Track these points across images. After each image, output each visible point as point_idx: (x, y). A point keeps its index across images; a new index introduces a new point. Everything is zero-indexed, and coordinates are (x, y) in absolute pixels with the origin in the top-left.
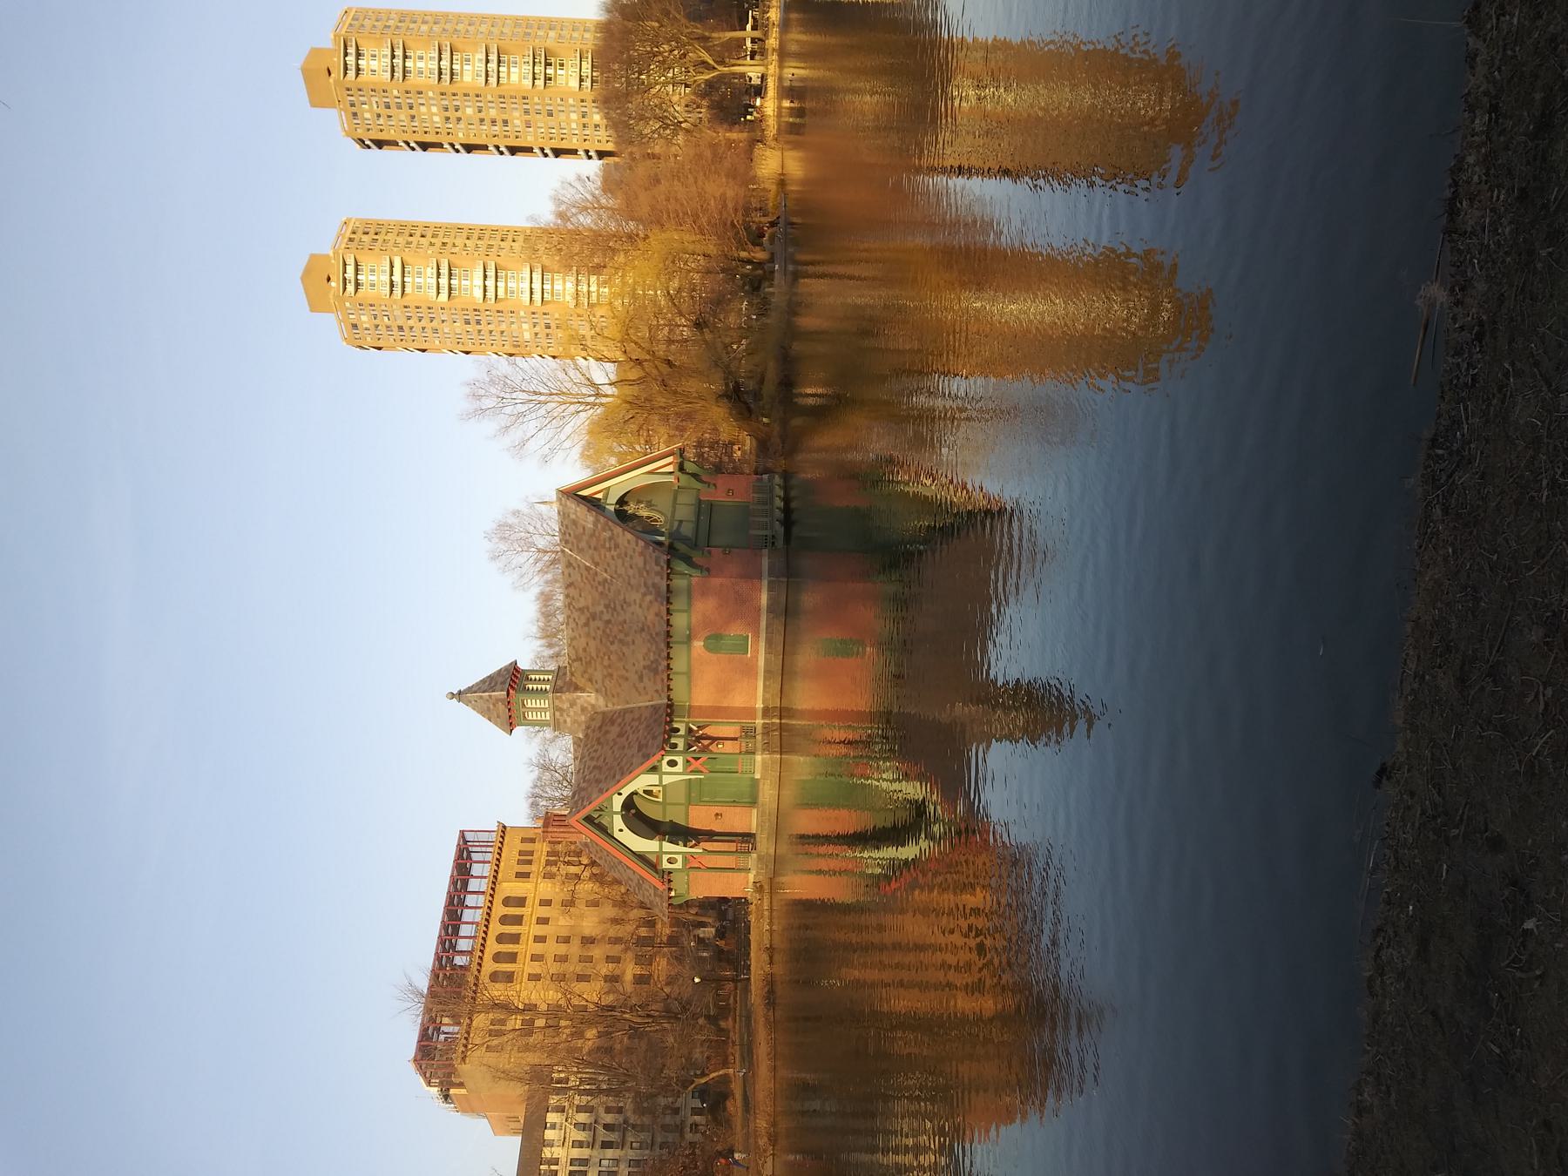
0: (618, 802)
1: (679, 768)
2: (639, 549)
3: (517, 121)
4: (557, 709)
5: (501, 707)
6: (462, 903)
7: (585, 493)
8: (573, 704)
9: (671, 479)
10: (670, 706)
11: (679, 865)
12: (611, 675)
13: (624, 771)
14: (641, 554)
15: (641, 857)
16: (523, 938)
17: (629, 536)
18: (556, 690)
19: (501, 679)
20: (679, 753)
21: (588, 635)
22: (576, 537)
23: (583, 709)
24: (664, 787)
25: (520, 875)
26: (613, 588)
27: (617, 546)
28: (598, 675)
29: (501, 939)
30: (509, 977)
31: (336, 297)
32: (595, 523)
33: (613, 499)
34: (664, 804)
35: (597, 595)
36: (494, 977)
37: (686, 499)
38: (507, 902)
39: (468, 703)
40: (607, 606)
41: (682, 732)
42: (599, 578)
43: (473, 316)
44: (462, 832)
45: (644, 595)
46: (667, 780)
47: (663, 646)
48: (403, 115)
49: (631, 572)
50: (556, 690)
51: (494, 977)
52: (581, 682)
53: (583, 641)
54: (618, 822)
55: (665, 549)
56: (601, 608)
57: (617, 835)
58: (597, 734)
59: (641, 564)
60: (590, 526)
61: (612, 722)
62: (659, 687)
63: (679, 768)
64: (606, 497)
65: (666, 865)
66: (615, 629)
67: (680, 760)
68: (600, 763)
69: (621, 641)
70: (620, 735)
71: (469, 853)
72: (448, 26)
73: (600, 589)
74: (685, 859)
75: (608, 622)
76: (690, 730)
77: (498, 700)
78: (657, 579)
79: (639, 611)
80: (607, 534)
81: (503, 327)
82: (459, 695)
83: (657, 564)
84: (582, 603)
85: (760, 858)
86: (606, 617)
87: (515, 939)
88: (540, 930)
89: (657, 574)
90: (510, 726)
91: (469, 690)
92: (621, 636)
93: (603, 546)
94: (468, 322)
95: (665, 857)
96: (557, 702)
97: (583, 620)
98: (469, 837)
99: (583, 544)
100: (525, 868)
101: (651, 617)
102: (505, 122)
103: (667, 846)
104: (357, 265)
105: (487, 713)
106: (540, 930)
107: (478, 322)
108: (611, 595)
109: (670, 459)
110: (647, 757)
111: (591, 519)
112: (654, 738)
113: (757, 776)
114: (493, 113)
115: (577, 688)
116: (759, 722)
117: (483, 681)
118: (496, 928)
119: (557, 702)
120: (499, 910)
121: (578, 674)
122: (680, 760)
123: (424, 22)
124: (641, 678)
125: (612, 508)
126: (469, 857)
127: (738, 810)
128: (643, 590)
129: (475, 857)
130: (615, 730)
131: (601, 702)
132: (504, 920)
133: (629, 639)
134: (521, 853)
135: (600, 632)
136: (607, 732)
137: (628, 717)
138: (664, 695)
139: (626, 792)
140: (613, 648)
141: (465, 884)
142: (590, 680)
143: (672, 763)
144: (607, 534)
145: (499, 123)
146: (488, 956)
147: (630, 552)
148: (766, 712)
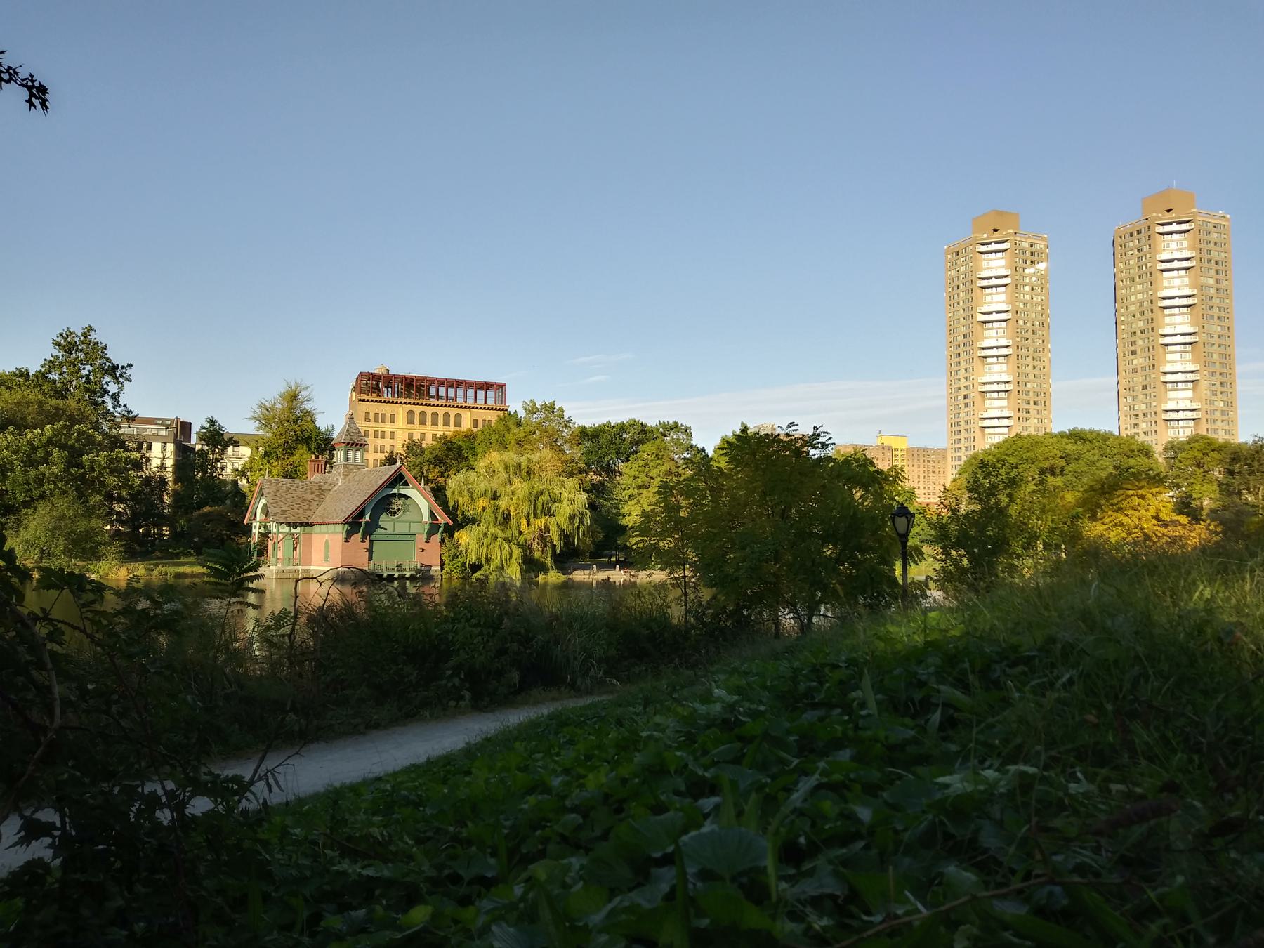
3: (1138, 361)
10: (307, 525)
25: (476, 421)
29: (435, 414)
30: (411, 422)
31: (976, 238)
33: (402, 491)
36: (411, 413)
38: (458, 416)
43: (968, 340)
48: (1134, 272)
50: (345, 466)
51: (411, 413)
72: (1216, 301)
81: (963, 363)
94: (965, 336)
102: (1134, 353)
104: (1003, 251)
107: (965, 345)
114: (1140, 342)
116: (300, 568)
120: (453, 412)
123: (1217, 281)
125: (395, 491)
145: (1133, 348)
148: (308, 571)
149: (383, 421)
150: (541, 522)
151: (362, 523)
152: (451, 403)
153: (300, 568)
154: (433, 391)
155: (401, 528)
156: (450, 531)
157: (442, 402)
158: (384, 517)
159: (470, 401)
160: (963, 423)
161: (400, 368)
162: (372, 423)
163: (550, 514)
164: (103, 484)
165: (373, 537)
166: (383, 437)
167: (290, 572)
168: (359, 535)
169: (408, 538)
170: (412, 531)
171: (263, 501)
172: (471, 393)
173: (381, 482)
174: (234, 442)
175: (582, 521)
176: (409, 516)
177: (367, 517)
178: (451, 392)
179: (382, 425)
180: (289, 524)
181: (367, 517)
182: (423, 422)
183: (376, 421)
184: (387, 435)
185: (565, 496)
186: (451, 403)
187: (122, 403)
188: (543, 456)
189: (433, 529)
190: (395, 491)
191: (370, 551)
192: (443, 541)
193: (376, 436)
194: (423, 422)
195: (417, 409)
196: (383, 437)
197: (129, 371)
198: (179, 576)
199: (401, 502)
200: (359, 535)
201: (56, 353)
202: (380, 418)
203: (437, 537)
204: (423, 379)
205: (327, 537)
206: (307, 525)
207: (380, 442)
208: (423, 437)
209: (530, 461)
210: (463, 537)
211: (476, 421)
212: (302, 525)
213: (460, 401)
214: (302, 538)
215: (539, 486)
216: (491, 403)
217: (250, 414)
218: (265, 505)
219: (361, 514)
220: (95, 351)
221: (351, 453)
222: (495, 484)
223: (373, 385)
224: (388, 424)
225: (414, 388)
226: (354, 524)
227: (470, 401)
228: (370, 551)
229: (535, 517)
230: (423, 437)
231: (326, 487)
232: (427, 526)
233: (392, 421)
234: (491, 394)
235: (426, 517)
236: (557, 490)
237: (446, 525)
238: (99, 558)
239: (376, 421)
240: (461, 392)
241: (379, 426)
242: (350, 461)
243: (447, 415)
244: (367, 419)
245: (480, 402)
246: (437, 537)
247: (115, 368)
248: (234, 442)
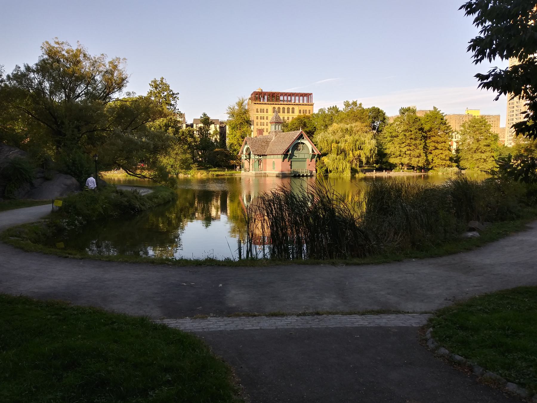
10: (265, 155)
25: (300, 110)
29: (284, 108)
33: (302, 141)
36: (274, 108)
37: (306, 156)
38: (293, 109)
44: (311, 94)
50: (275, 132)
70: (262, 146)
100: (302, 112)
116: (263, 172)
120: (291, 107)
125: (299, 141)
132: (288, 109)
134: (306, 110)
148: (265, 173)
149: (263, 112)
150: (358, 152)
151: (288, 155)
152: (289, 103)
153: (263, 172)
154: (281, 98)
155: (302, 156)
156: (319, 156)
157: (286, 103)
158: (295, 152)
159: (297, 102)
160: (515, 103)
161: (268, 89)
162: (259, 113)
163: (360, 149)
164: (187, 141)
165: (292, 160)
166: (263, 119)
167: (259, 173)
168: (287, 159)
169: (304, 160)
171: (246, 147)
172: (297, 98)
173: (295, 138)
174: (212, 123)
175: (374, 152)
176: (304, 151)
177: (290, 152)
178: (289, 98)
179: (262, 114)
180: (258, 155)
181: (290, 152)
182: (288, 112)
183: (261, 112)
184: (265, 118)
185: (367, 141)
186: (289, 103)
187: (177, 108)
188: (357, 125)
189: (314, 156)
190: (299, 141)
191: (291, 165)
192: (317, 161)
193: (261, 119)
194: (288, 112)
195: (277, 106)
196: (263, 119)
197: (178, 96)
198: (217, 175)
199: (301, 145)
200: (287, 159)
201: (151, 89)
202: (262, 111)
203: (314, 160)
204: (278, 93)
205: (274, 160)
206: (265, 155)
207: (262, 121)
208: (288, 118)
209: (352, 127)
210: (325, 159)
211: (300, 110)
212: (263, 155)
213: (293, 101)
214: (263, 161)
215: (357, 137)
216: (305, 102)
217: (226, 112)
218: (248, 149)
219: (288, 151)
220: (166, 87)
221: (277, 126)
222: (336, 137)
223: (258, 96)
224: (265, 113)
225: (274, 97)
226: (286, 155)
228: (291, 165)
229: (356, 151)
230: (288, 118)
231: (268, 140)
232: (311, 155)
233: (267, 112)
234: (305, 98)
235: (311, 152)
236: (363, 139)
237: (318, 154)
238: (190, 169)
239: (261, 112)
240: (293, 98)
241: (262, 114)
242: (277, 129)
243: (288, 109)
244: (257, 112)
245: (301, 102)
246: (314, 160)
247: (173, 94)
248: (212, 123)
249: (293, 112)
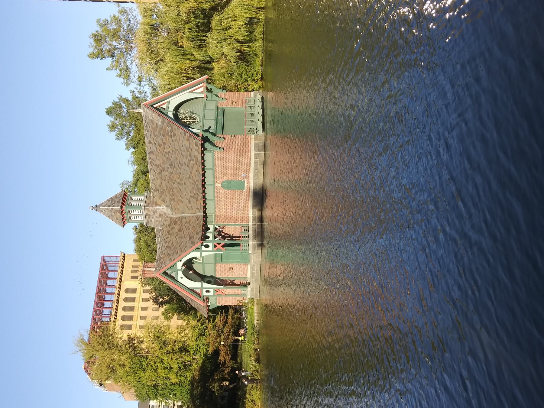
0: (180, 265)
1: (211, 248)
2: (186, 137)
4: (147, 215)
5: (119, 215)
6: (104, 291)
7: (155, 106)
8: (155, 212)
9: (202, 95)
11: (211, 293)
12: (174, 199)
13: (183, 250)
14: (188, 140)
15: (192, 290)
16: (136, 309)
17: (181, 130)
18: (147, 205)
19: (117, 200)
20: (210, 242)
21: (161, 178)
22: (153, 128)
23: (160, 215)
24: (203, 258)
25: (133, 278)
26: (173, 156)
27: (174, 135)
28: (167, 199)
29: (124, 309)
32: (163, 123)
33: (172, 108)
34: (203, 263)
35: (165, 159)
37: (212, 106)
38: (127, 291)
39: (101, 211)
40: (171, 165)
41: (211, 230)
42: (166, 150)
44: (103, 258)
45: (190, 160)
46: (204, 254)
47: (200, 187)
49: (182, 149)
51: (122, 327)
52: (159, 201)
53: (159, 182)
54: (180, 274)
55: (200, 138)
56: (168, 165)
57: (180, 280)
58: (168, 229)
59: (188, 145)
60: (160, 123)
61: (176, 223)
62: (199, 207)
63: (211, 248)
64: (168, 107)
65: (205, 294)
66: (175, 177)
67: (211, 245)
68: (170, 245)
69: (178, 183)
70: (180, 230)
71: (107, 267)
73: (167, 156)
74: (216, 291)
75: (172, 173)
76: (216, 229)
77: (116, 211)
78: (196, 153)
79: (187, 169)
80: (169, 129)
82: (96, 208)
83: (196, 145)
84: (158, 162)
85: (252, 290)
86: (170, 170)
87: (132, 309)
88: (144, 313)
89: (196, 150)
90: (124, 223)
91: (101, 205)
92: (178, 180)
93: (168, 134)
95: (205, 290)
96: (147, 212)
97: (159, 171)
98: (107, 259)
99: (157, 133)
100: (135, 274)
101: (194, 172)
103: (206, 285)
105: (111, 217)
106: (144, 313)
108: (173, 159)
109: (202, 85)
110: (193, 243)
111: (160, 120)
112: (197, 234)
113: (250, 252)
115: (157, 204)
117: (108, 201)
118: (122, 304)
119: (147, 212)
120: (123, 295)
121: (157, 197)
122: (211, 245)
124: (190, 202)
126: (107, 269)
127: (240, 266)
128: (189, 158)
129: (110, 268)
130: (177, 227)
131: (169, 212)
132: (126, 300)
133: (183, 182)
134: (133, 267)
135: (167, 178)
136: (173, 228)
137: (184, 221)
138: (202, 210)
139: (184, 260)
140: (175, 186)
141: (102, 304)
142: (163, 201)
143: (207, 246)
144: (169, 129)
146: (119, 317)
147: (182, 139)
155: (211, 115)
170: (214, 108)
205: (218, 185)
227: (116, 282)
231: (167, 223)
249: (134, 291)
